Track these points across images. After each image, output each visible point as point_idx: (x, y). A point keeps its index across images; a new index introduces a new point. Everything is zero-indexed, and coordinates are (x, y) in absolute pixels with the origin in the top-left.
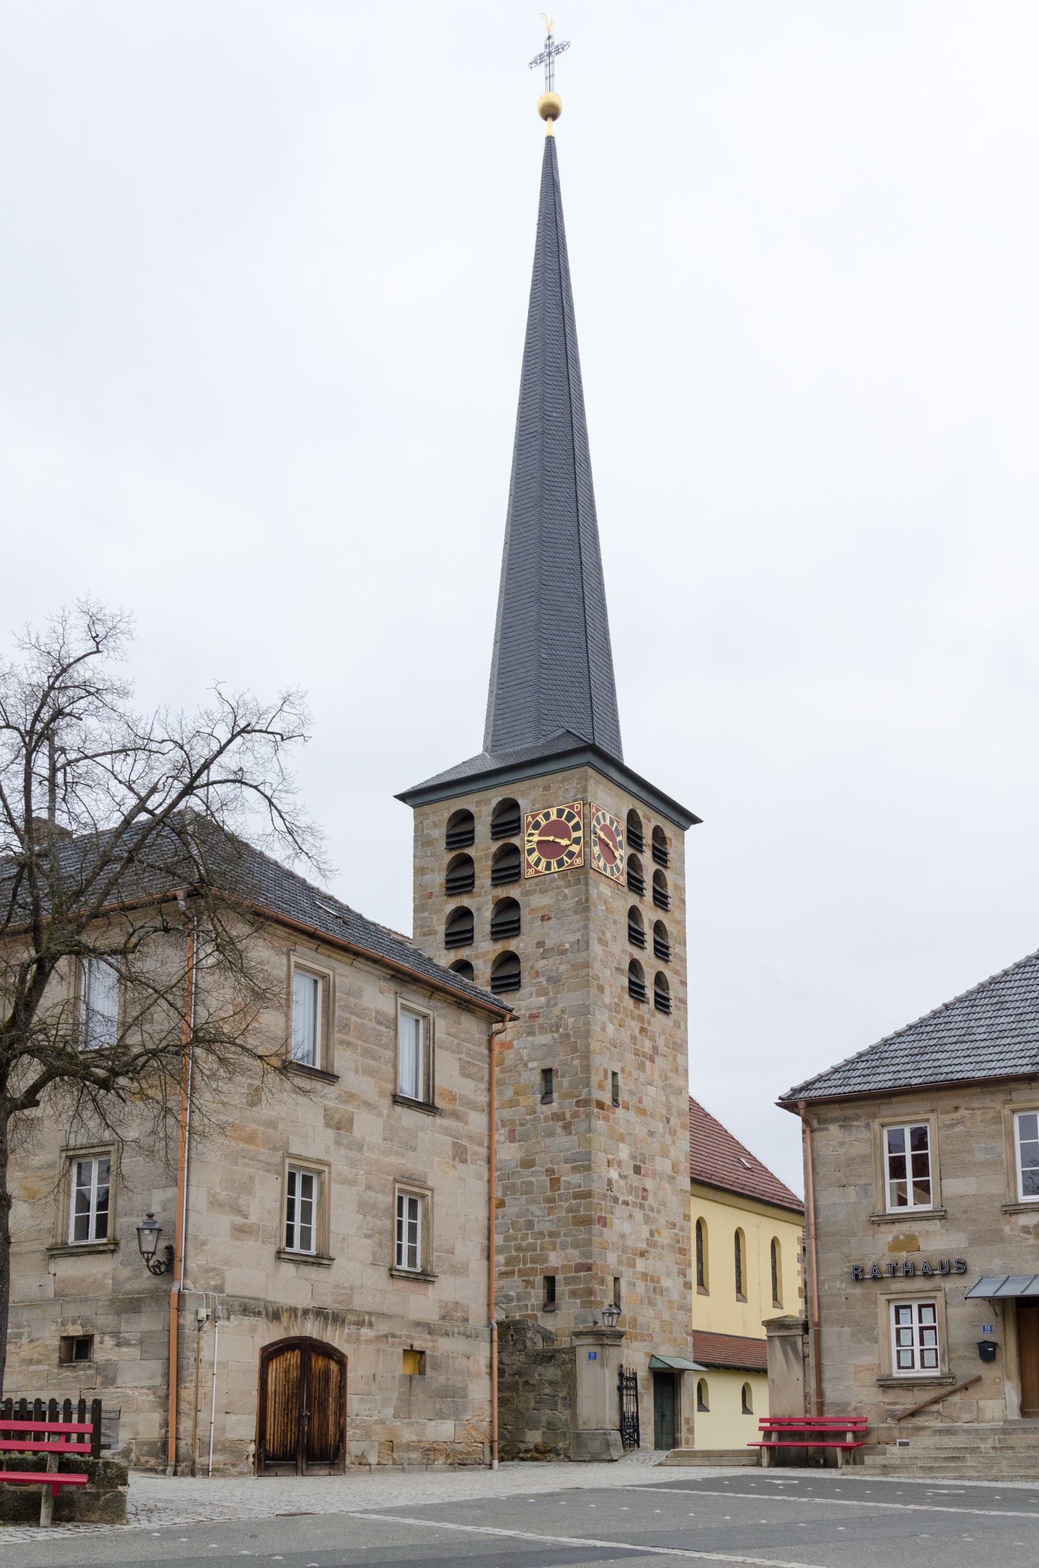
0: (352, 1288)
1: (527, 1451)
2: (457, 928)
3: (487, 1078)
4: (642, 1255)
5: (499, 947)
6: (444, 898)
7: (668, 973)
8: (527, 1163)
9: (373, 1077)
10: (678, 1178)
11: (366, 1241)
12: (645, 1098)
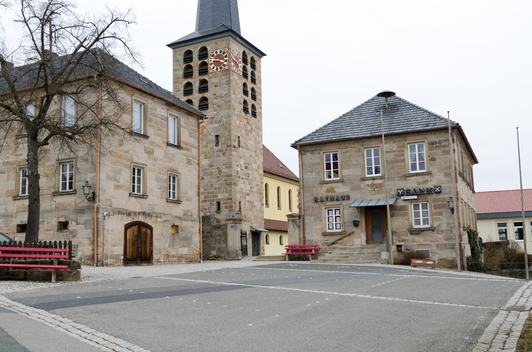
0: (154, 205)
1: (212, 257)
4: (248, 195)
5: (201, 95)
8: (211, 166)
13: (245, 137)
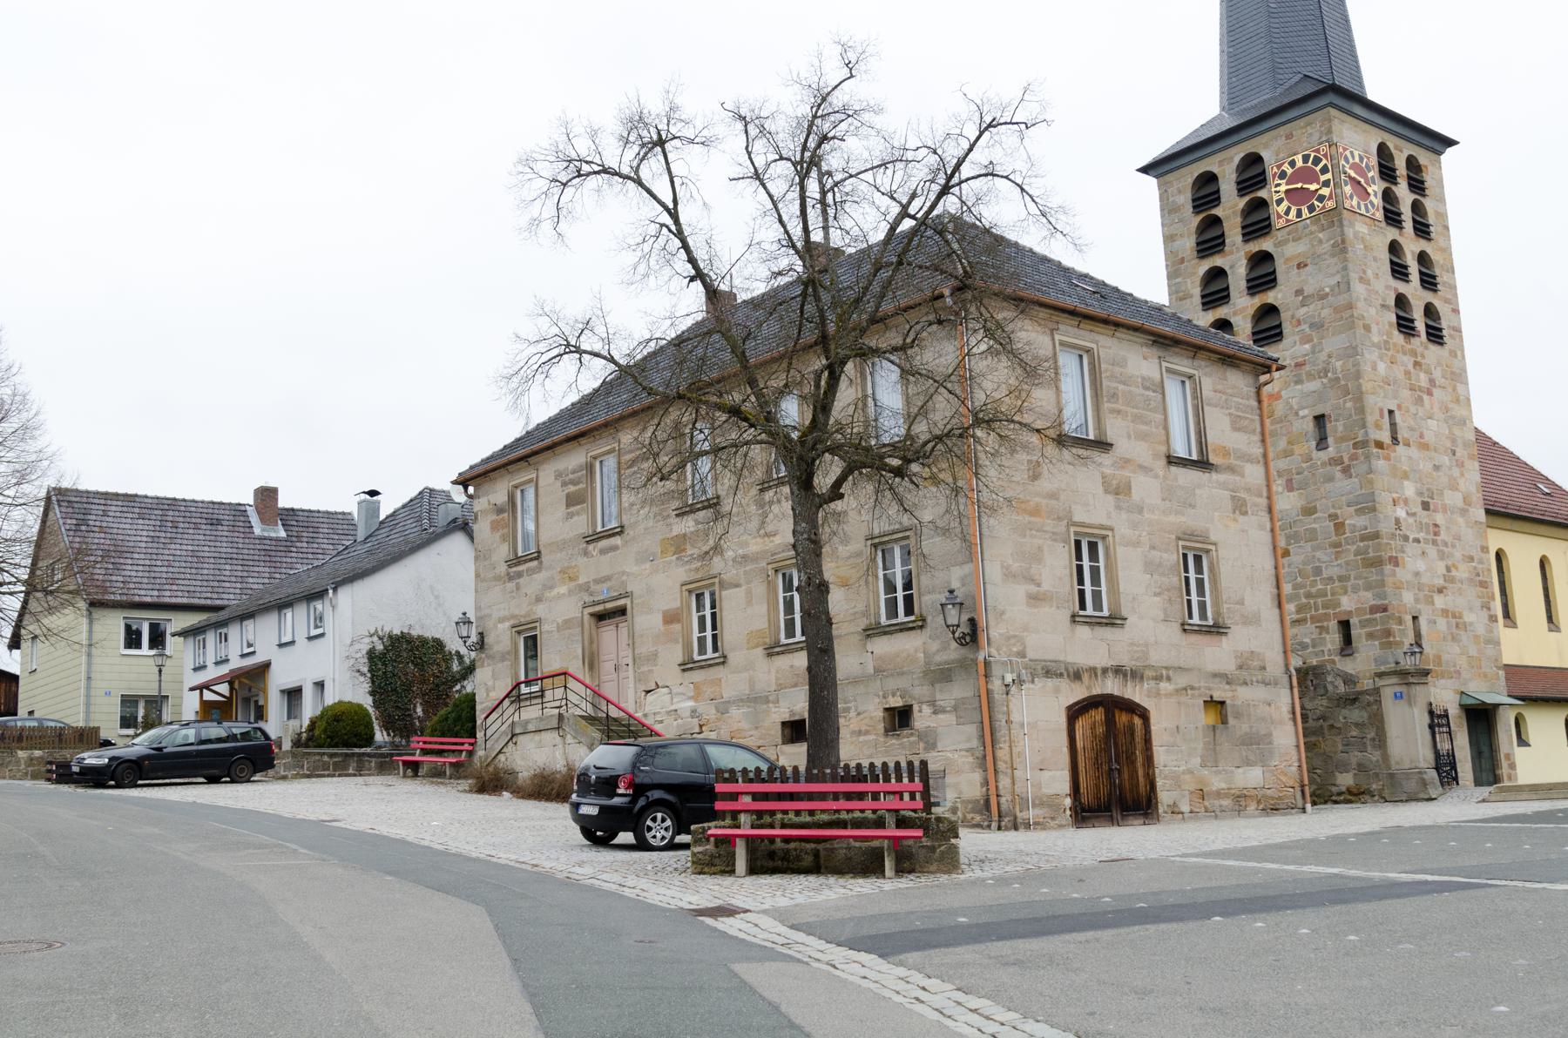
2: (1213, 288)
3: (1259, 430)
4: (1440, 591)
5: (1257, 301)
7: (1437, 303)
8: (1309, 511)
13: (1413, 409)
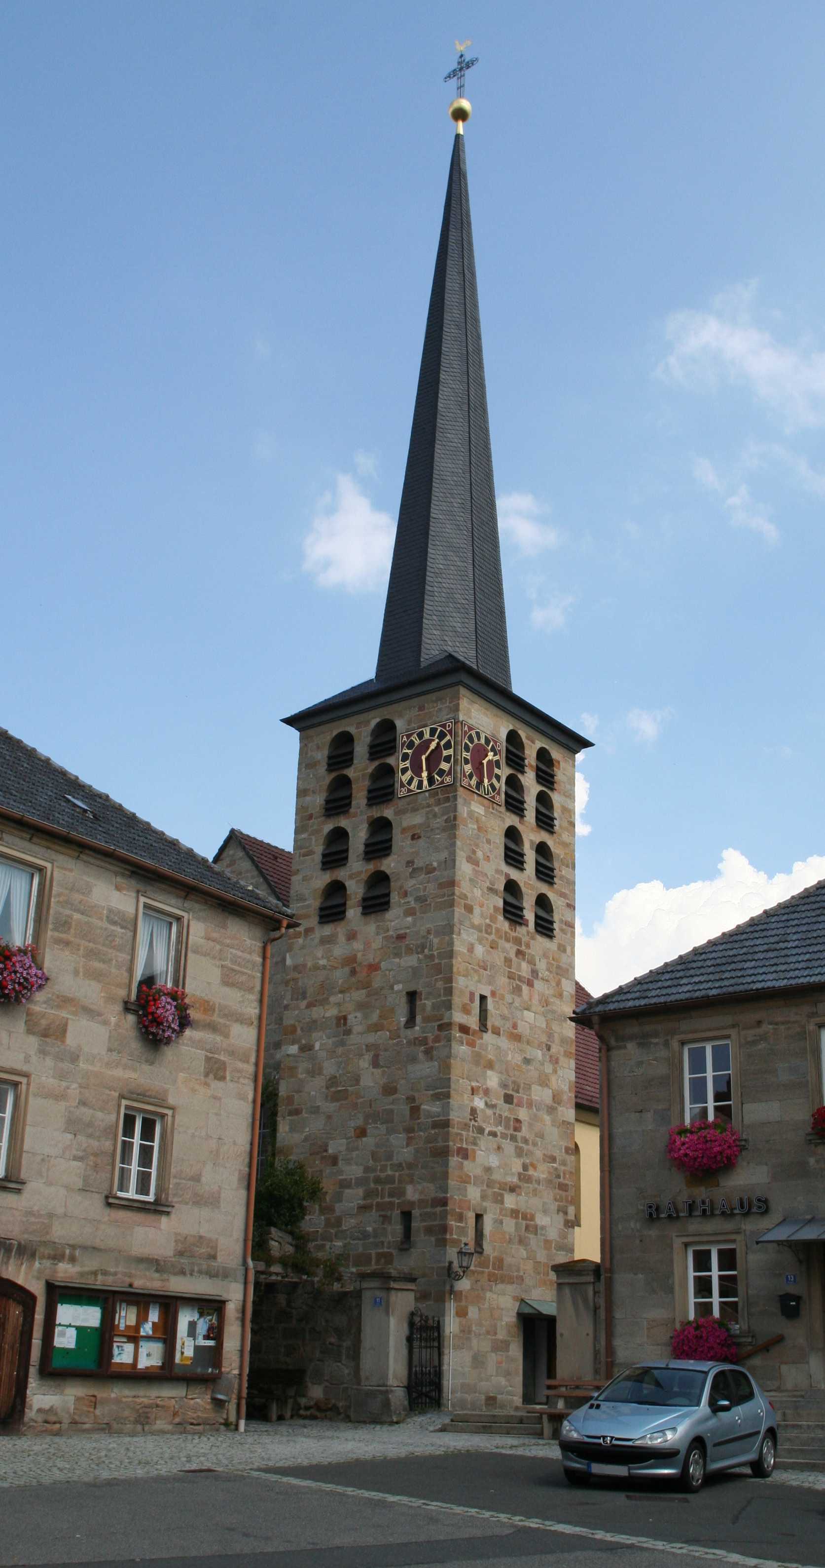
0: (51, 1215)
1: (307, 1408)
2: (334, 849)
3: (258, 988)
4: (512, 1189)
5: (371, 867)
6: (323, 818)
7: (551, 895)
8: (389, 1090)
9: (99, 981)
10: (560, 1109)
11: (75, 1163)
12: (520, 1024)
13: (509, 998)
